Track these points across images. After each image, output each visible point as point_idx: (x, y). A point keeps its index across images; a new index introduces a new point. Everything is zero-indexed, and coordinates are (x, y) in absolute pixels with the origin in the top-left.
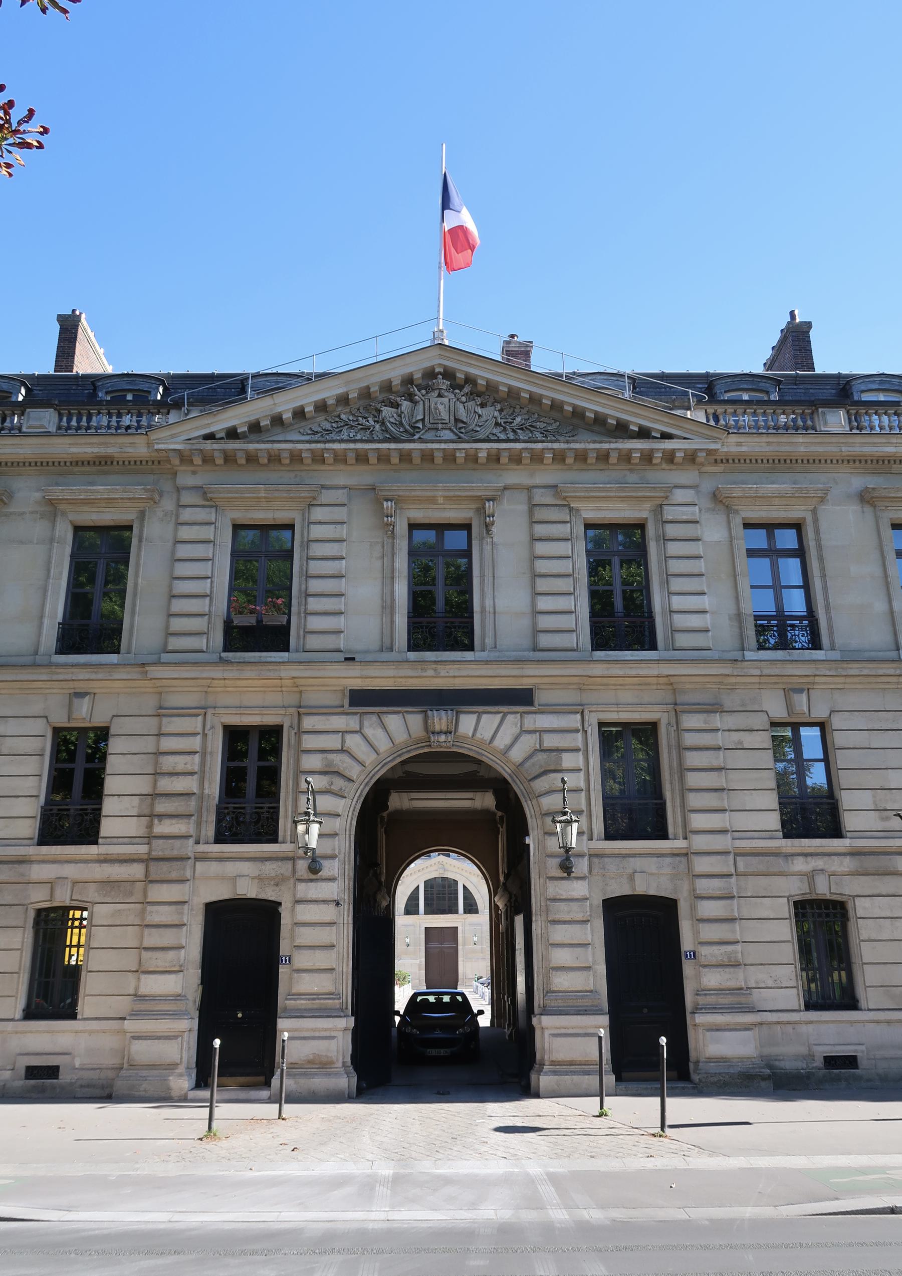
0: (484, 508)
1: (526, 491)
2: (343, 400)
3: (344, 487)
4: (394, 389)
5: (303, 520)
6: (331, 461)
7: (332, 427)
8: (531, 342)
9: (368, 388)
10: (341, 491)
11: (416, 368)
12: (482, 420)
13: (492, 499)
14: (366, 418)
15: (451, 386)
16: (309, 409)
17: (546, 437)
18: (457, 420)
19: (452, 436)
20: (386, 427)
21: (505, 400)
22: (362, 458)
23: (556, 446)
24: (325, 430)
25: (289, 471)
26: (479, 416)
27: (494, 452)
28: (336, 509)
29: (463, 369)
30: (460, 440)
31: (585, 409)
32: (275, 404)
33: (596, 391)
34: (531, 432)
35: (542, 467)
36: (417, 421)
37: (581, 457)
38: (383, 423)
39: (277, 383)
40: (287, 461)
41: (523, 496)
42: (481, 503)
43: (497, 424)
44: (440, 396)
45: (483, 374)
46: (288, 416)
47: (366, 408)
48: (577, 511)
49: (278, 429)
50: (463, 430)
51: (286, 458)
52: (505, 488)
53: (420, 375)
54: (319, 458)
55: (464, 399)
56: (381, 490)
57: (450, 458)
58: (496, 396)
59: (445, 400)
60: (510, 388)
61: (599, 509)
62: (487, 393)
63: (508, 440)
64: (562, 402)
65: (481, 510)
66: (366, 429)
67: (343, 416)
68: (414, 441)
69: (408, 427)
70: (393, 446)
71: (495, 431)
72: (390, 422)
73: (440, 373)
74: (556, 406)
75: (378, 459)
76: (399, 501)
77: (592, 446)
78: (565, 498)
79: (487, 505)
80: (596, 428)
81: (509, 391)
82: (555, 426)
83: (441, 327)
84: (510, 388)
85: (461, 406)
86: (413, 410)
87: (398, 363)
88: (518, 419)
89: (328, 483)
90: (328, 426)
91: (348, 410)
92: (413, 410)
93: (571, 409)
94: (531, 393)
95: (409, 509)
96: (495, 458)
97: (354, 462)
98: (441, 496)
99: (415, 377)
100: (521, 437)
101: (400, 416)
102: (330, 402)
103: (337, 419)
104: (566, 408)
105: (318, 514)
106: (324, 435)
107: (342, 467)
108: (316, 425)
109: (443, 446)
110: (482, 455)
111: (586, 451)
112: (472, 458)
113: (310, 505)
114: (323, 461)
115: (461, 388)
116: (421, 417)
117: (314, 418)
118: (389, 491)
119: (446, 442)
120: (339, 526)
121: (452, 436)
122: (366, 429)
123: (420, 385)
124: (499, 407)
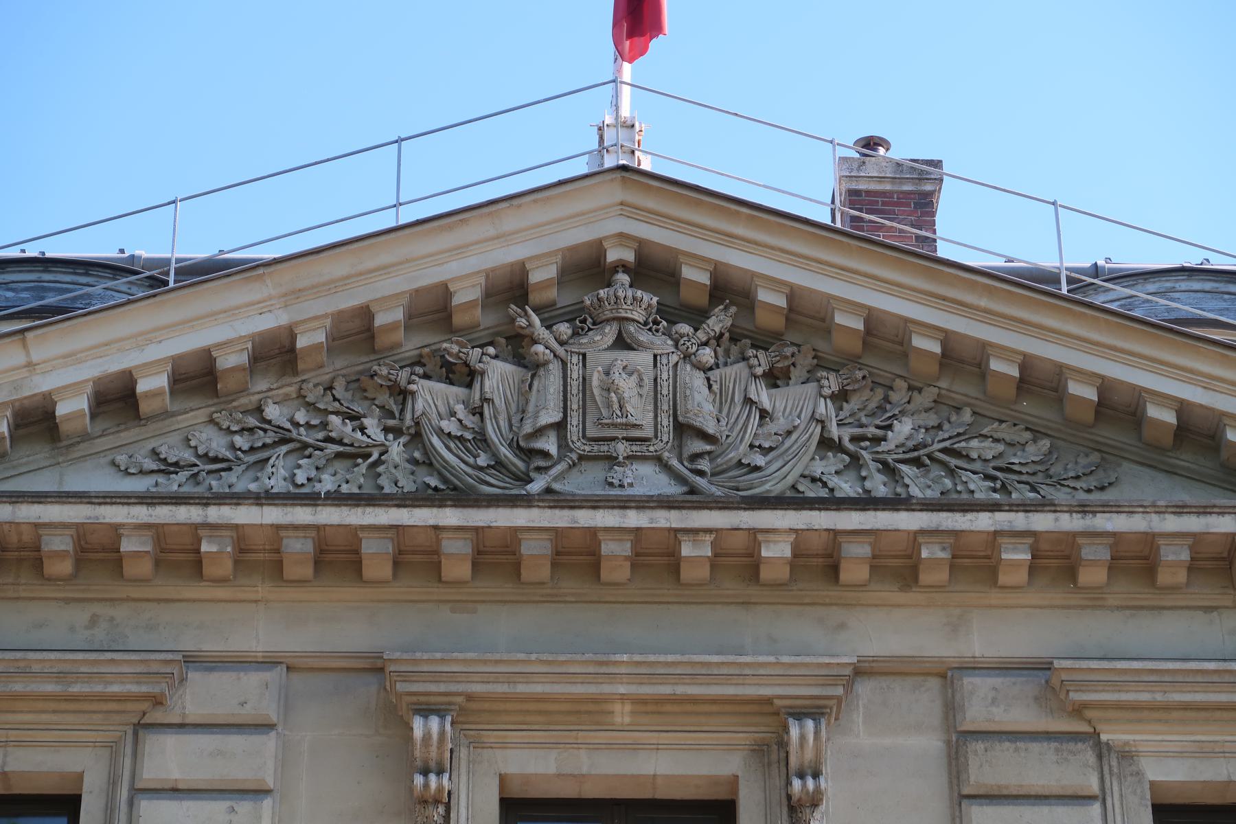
0: (783, 744)
1: (934, 683)
2: (277, 354)
3: (268, 663)
4: (458, 320)
5: (113, 782)
6: (227, 567)
7: (233, 447)
9: (365, 313)
10: (253, 679)
11: (538, 248)
12: (772, 427)
13: (813, 711)
14: (354, 417)
15: (662, 310)
16: (152, 383)
17: (1004, 489)
18: (683, 429)
19: (664, 486)
20: (428, 450)
21: (854, 360)
22: (337, 558)
23: (1042, 522)
24: (206, 458)
25: (67, 601)
26: (764, 414)
27: (817, 544)
28: (236, 742)
29: (701, 251)
30: (693, 499)
31: (1139, 396)
32: (30, 365)
33: (1178, 330)
34: (952, 472)
35: (995, 597)
36: (539, 432)
37: (1137, 561)
38: (417, 437)
39: (39, 290)
40: (66, 567)
41: (924, 701)
42: (771, 726)
43: (827, 444)
44: (622, 343)
45: (774, 272)
46: (72, 407)
47: (358, 384)
48: (1127, 755)
49: (38, 453)
50: (704, 465)
51: (61, 555)
52: (861, 671)
53: (551, 272)
54: (180, 557)
55: (707, 355)
56: (406, 677)
57: (658, 559)
58: (822, 345)
59: (642, 359)
60: (873, 321)
61: (1204, 752)
62: (790, 337)
63: (867, 502)
64: (1061, 372)
65: (772, 753)
66: (353, 455)
67: (272, 412)
68: (526, 501)
69: (505, 451)
70: (450, 517)
71: (818, 468)
72: (440, 432)
73: (623, 266)
74: (1039, 382)
75: (396, 564)
76: (467, 714)
77: (1171, 524)
78: (1078, 711)
79: (794, 732)
80: (1185, 459)
81: (869, 331)
82: (1035, 451)
83: (625, 112)
84: (872, 318)
85: (698, 380)
86: (525, 391)
87: (477, 229)
88: (903, 429)
89: (211, 645)
90: (217, 444)
91: (291, 390)
92: (525, 391)
93: (1091, 394)
94: (947, 338)
95: (504, 746)
96: (821, 563)
97: (308, 571)
98: (623, 698)
99: (535, 277)
100: (915, 491)
101: (478, 412)
102: (229, 360)
103: (252, 421)
104: (1075, 388)
105: (168, 757)
106: (203, 476)
107: (263, 590)
108: (175, 439)
109: (634, 519)
110: (777, 551)
111: (1150, 540)
112: (740, 563)
113: (141, 727)
114: (195, 566)
115: (697, 316)
116: (551, 415)
117: (166, 415)
118: (436, 677)
119: (642, 504)
120: (245, 807)
121: (664, 486)
122: (353, 455)
123: (551, 305)
124: (832, 383)
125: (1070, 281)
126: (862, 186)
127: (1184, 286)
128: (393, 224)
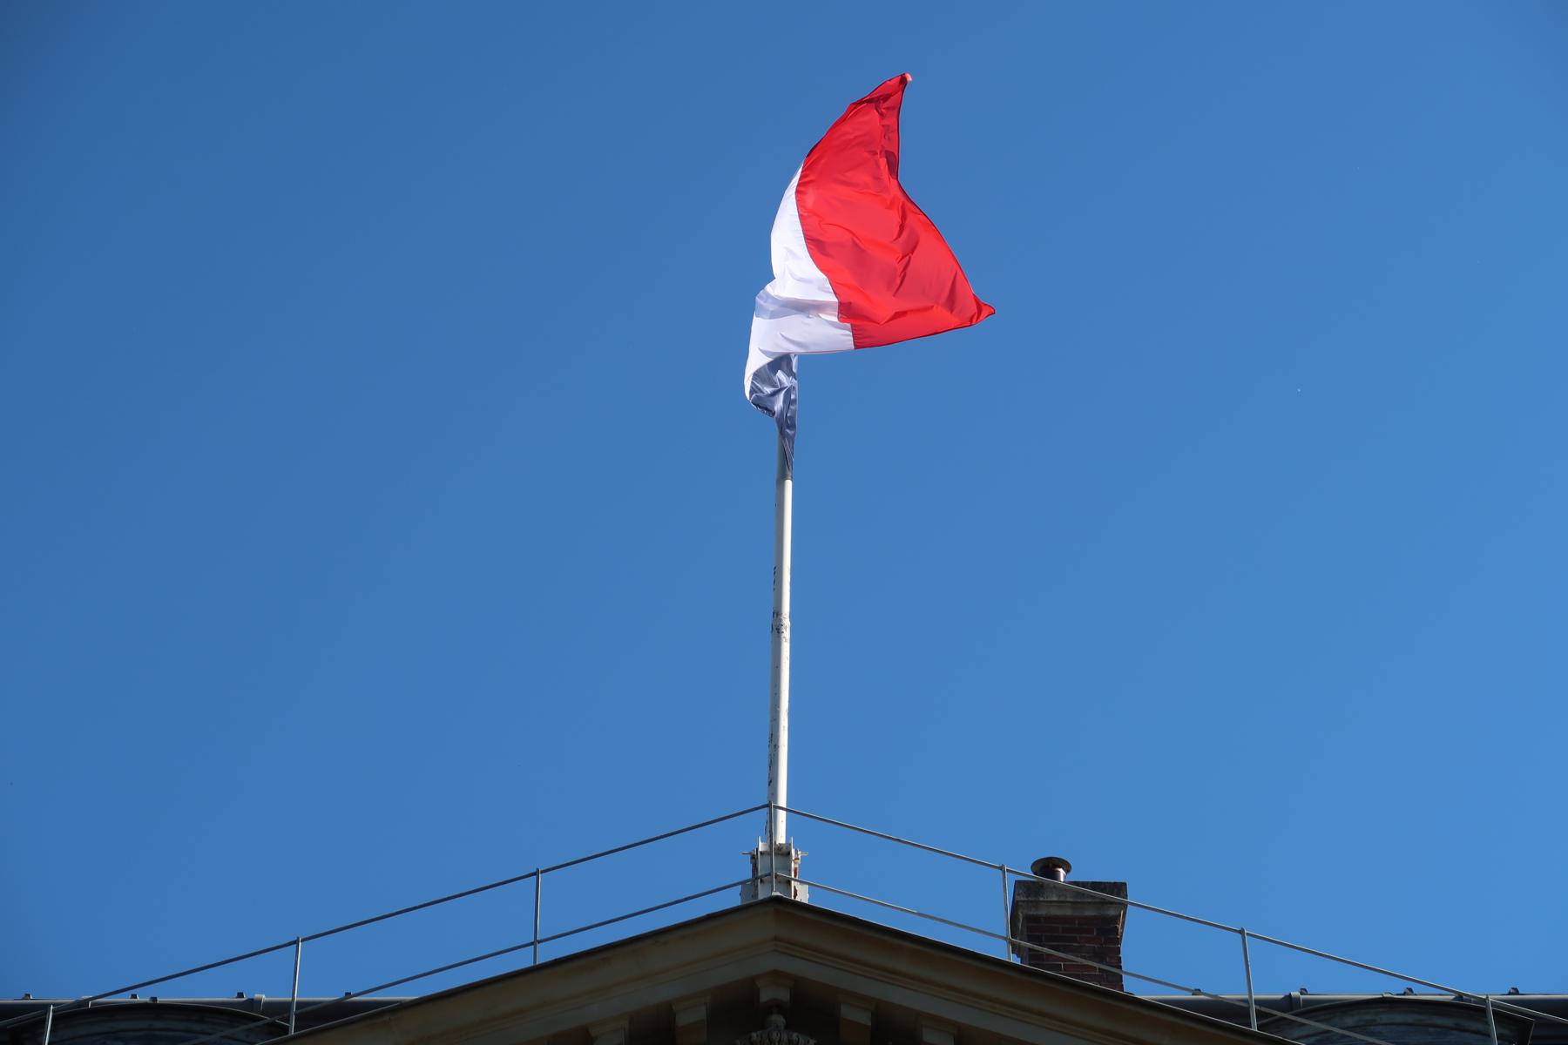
8: (1119, 888)
53: (698, 1014)
99: (684, 1020)
125: (1260, 1015)
126: (1042, 912)
127: (1385, 1018)
128: (530, 964)
